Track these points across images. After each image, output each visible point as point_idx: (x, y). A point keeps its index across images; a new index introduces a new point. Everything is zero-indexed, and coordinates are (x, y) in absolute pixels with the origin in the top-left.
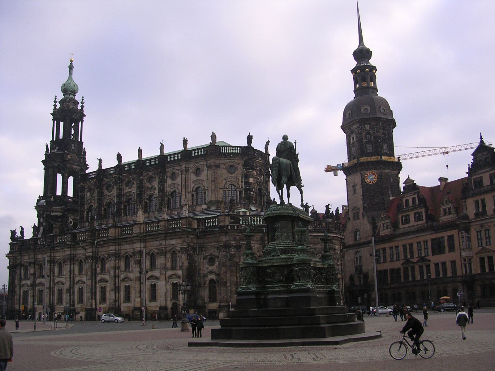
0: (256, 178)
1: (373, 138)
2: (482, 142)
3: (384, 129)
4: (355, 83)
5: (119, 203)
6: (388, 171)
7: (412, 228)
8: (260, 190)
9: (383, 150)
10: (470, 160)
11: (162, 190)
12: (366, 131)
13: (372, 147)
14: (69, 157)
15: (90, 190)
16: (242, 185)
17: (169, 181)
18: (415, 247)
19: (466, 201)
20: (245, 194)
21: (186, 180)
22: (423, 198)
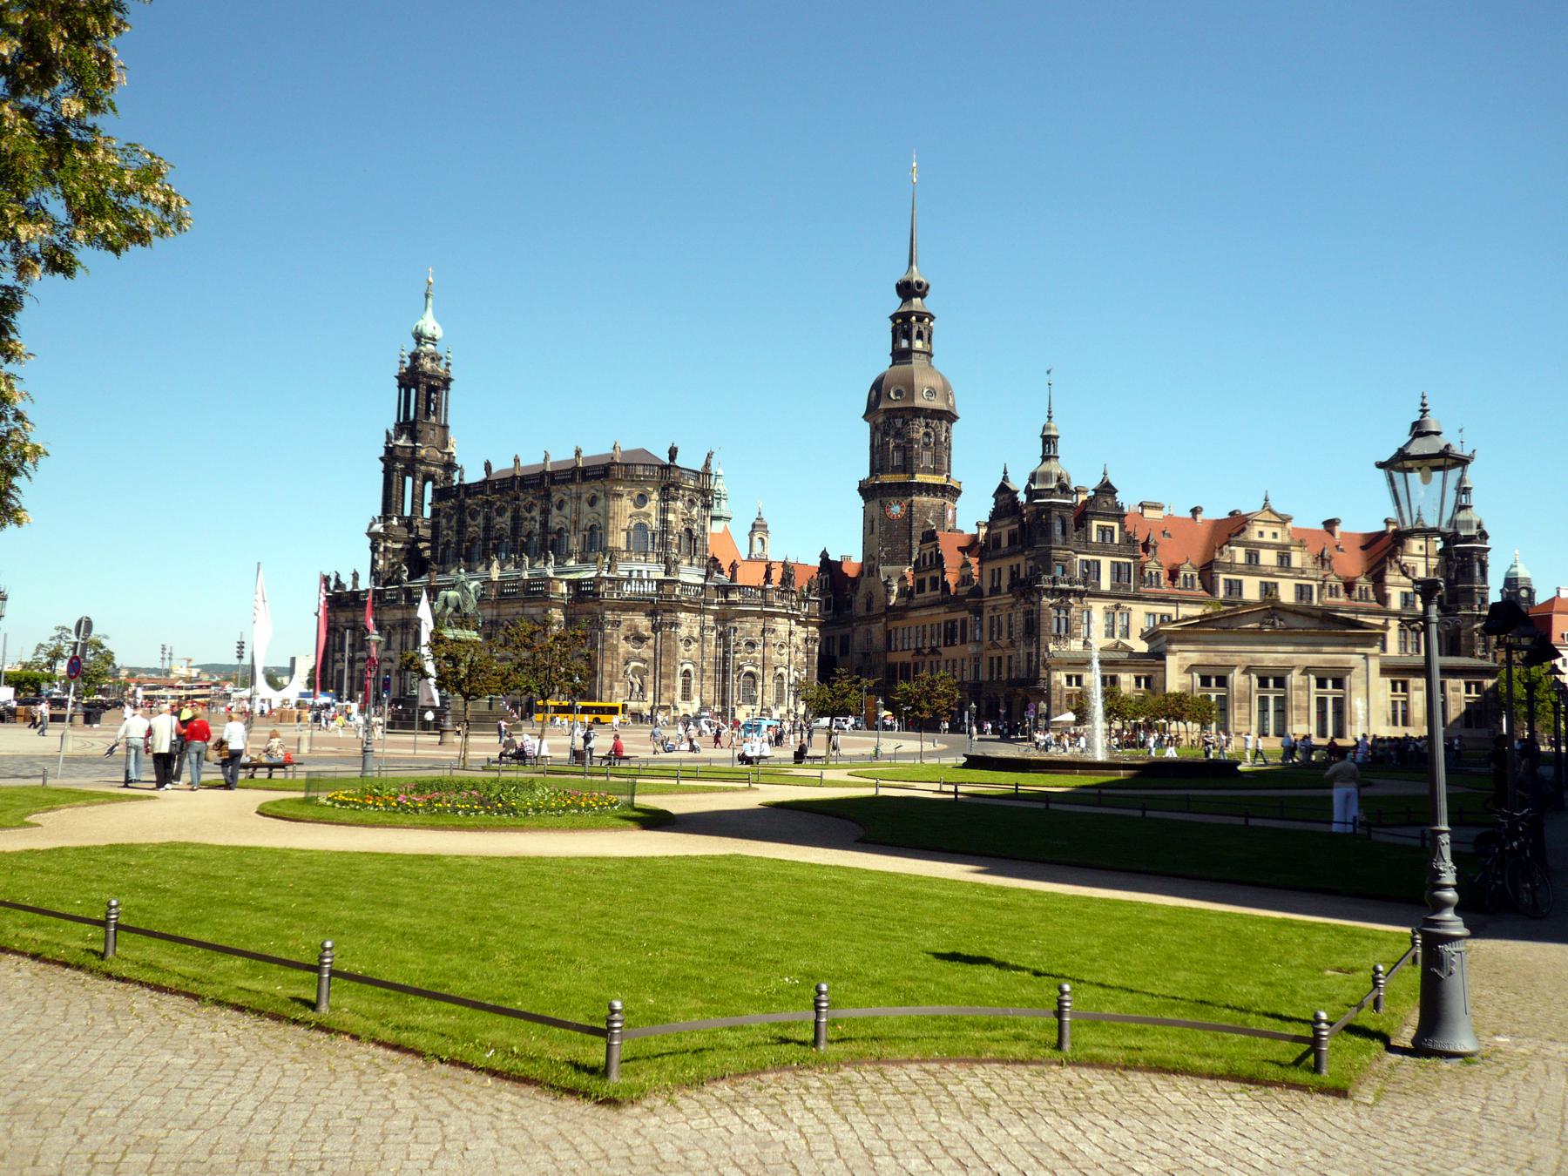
2: (1005, 478)
3: (927, 426)
4: (895, 340)
5: (487, 539)
8: (689, 531)
10: (990, 504)
11: (544, 524)
14: (423, 452)
15: (449, 517)
17: (554, 511)
18: (928, 629)
21: (578, 512)
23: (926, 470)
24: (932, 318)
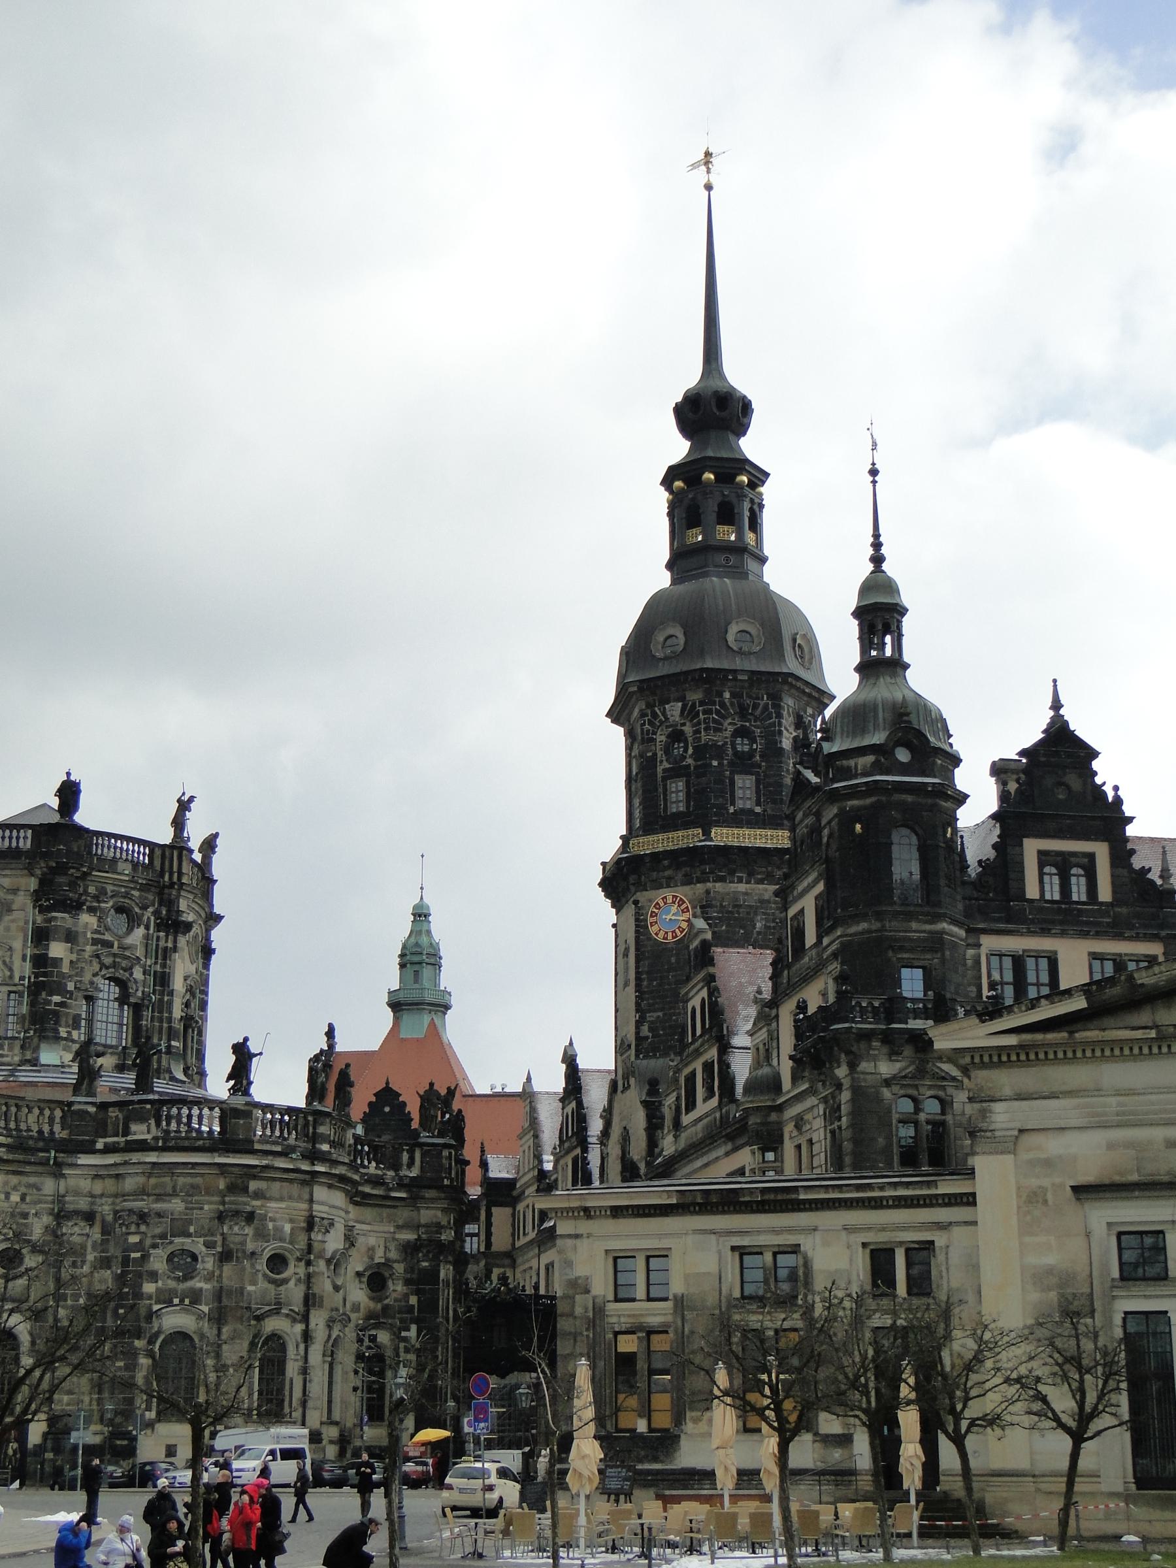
0: (95, 942)
1: (691, 756)
3: (743, 713)
6: (742, 887)
7: (700, 1126)
9: (733, 803)
12: (667, 727)
13: (688, 794)
16: (23, 969)
19: (777, 1016)
20: (33, 1004)
22: (716, 1001)
23: (744, 819)
24: (759, 477)
